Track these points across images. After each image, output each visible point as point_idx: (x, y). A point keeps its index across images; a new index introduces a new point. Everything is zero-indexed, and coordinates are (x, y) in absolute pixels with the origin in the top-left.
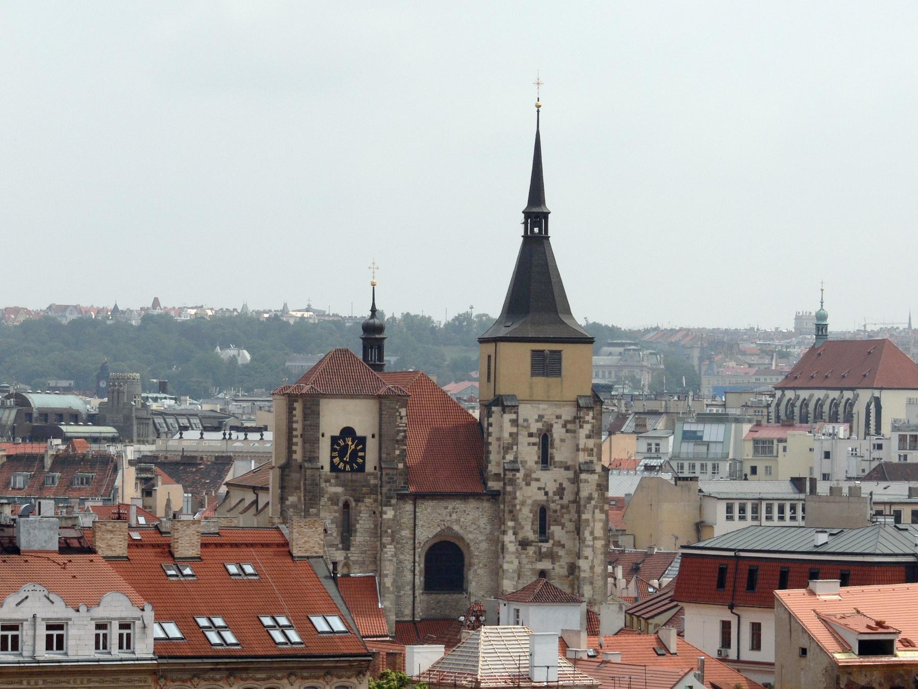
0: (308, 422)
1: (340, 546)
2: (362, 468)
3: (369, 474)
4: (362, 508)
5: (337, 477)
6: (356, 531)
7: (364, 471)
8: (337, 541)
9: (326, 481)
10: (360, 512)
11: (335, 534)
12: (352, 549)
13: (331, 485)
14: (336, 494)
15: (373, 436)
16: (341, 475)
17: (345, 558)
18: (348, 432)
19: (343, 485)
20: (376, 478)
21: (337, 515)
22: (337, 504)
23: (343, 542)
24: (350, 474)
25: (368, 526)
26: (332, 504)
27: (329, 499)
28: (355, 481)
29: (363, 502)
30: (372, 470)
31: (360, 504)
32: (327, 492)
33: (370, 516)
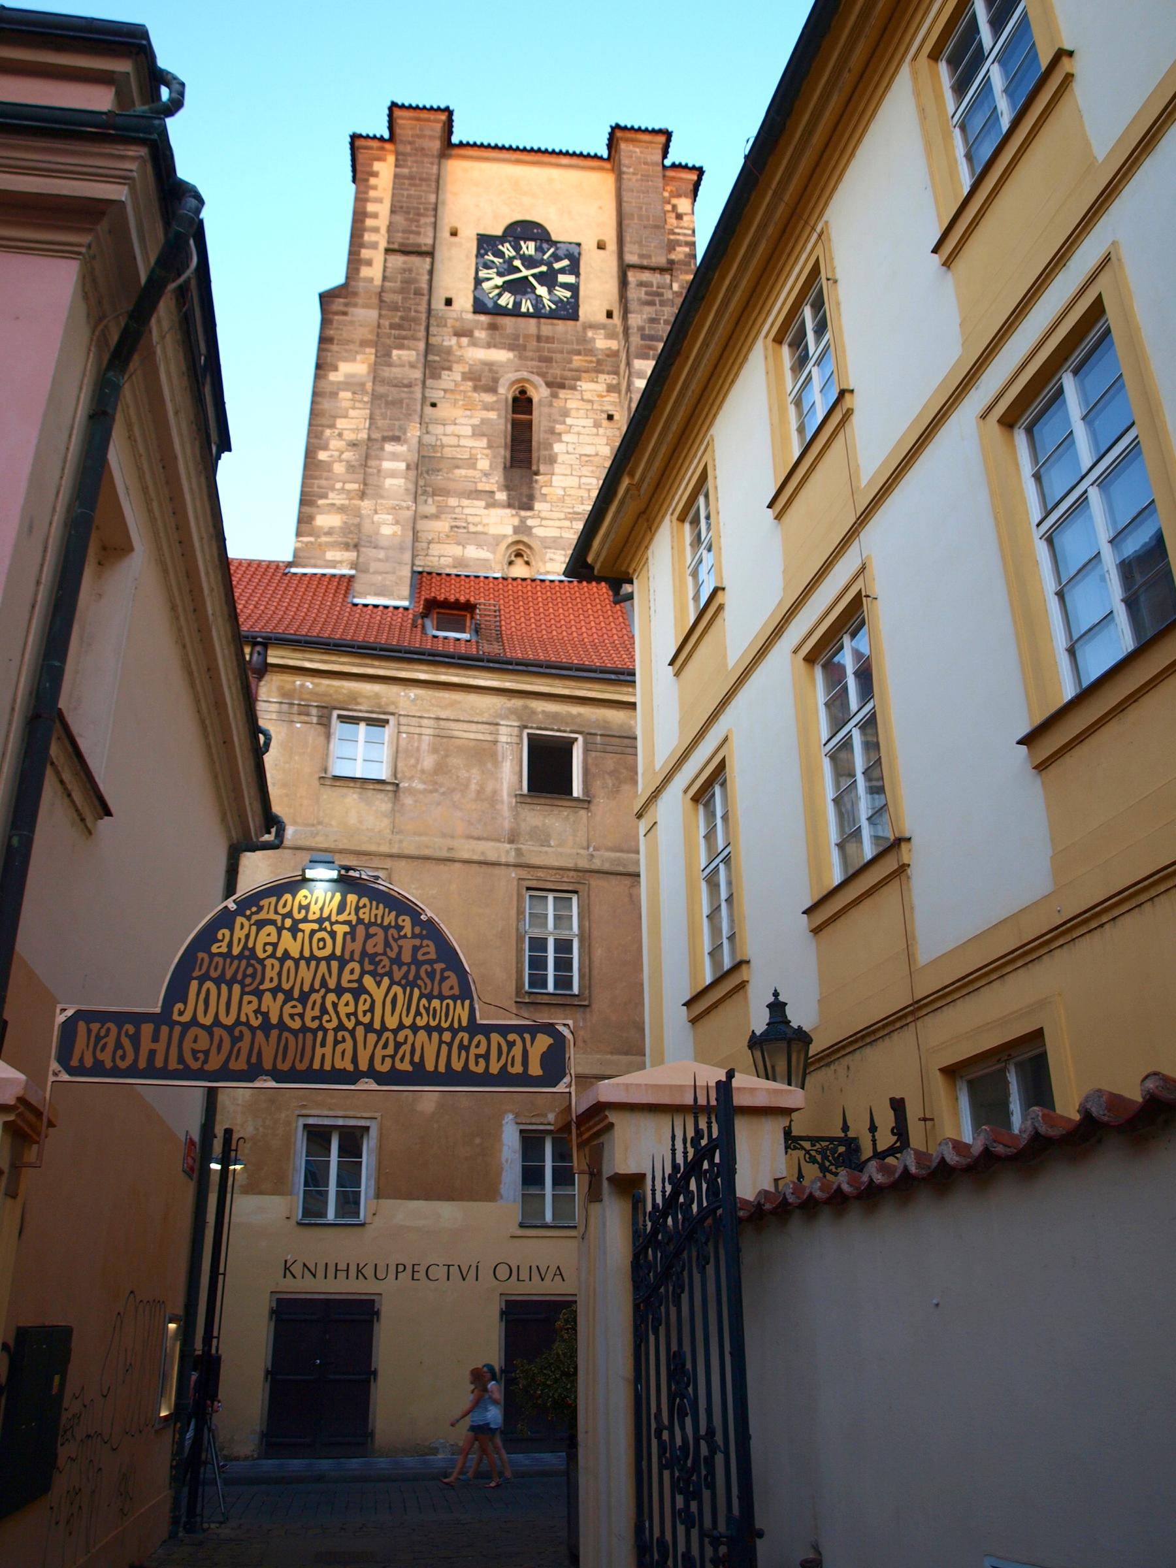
0: (406, 171)
1: (501, 496)
2: (569, 311)
3: (592, 326)
4: (571, 404)
5: (493, 327)
6: (552, 460)
7: (575, 317)
8: (494, 482)
9: (458, 334)
10: (565, 413)
11: (484, 464)
12: (538, 506)
13: (474, 344)
14: (490, 365)
15: (601, 246)
16: (508, 322)
17: (517, 530)
18: (522, 230)
19: (513, 345)
20: (611, 336)
21: (493, 415)
22: (493, 390)
24: (533, 321)
25: (589, 450)
26: (476, 389)
27: (466, 377)
29: (574, 388)
30: (601, 317)
31: (562, 394)
32: (460, 360)
33: (597, 425)
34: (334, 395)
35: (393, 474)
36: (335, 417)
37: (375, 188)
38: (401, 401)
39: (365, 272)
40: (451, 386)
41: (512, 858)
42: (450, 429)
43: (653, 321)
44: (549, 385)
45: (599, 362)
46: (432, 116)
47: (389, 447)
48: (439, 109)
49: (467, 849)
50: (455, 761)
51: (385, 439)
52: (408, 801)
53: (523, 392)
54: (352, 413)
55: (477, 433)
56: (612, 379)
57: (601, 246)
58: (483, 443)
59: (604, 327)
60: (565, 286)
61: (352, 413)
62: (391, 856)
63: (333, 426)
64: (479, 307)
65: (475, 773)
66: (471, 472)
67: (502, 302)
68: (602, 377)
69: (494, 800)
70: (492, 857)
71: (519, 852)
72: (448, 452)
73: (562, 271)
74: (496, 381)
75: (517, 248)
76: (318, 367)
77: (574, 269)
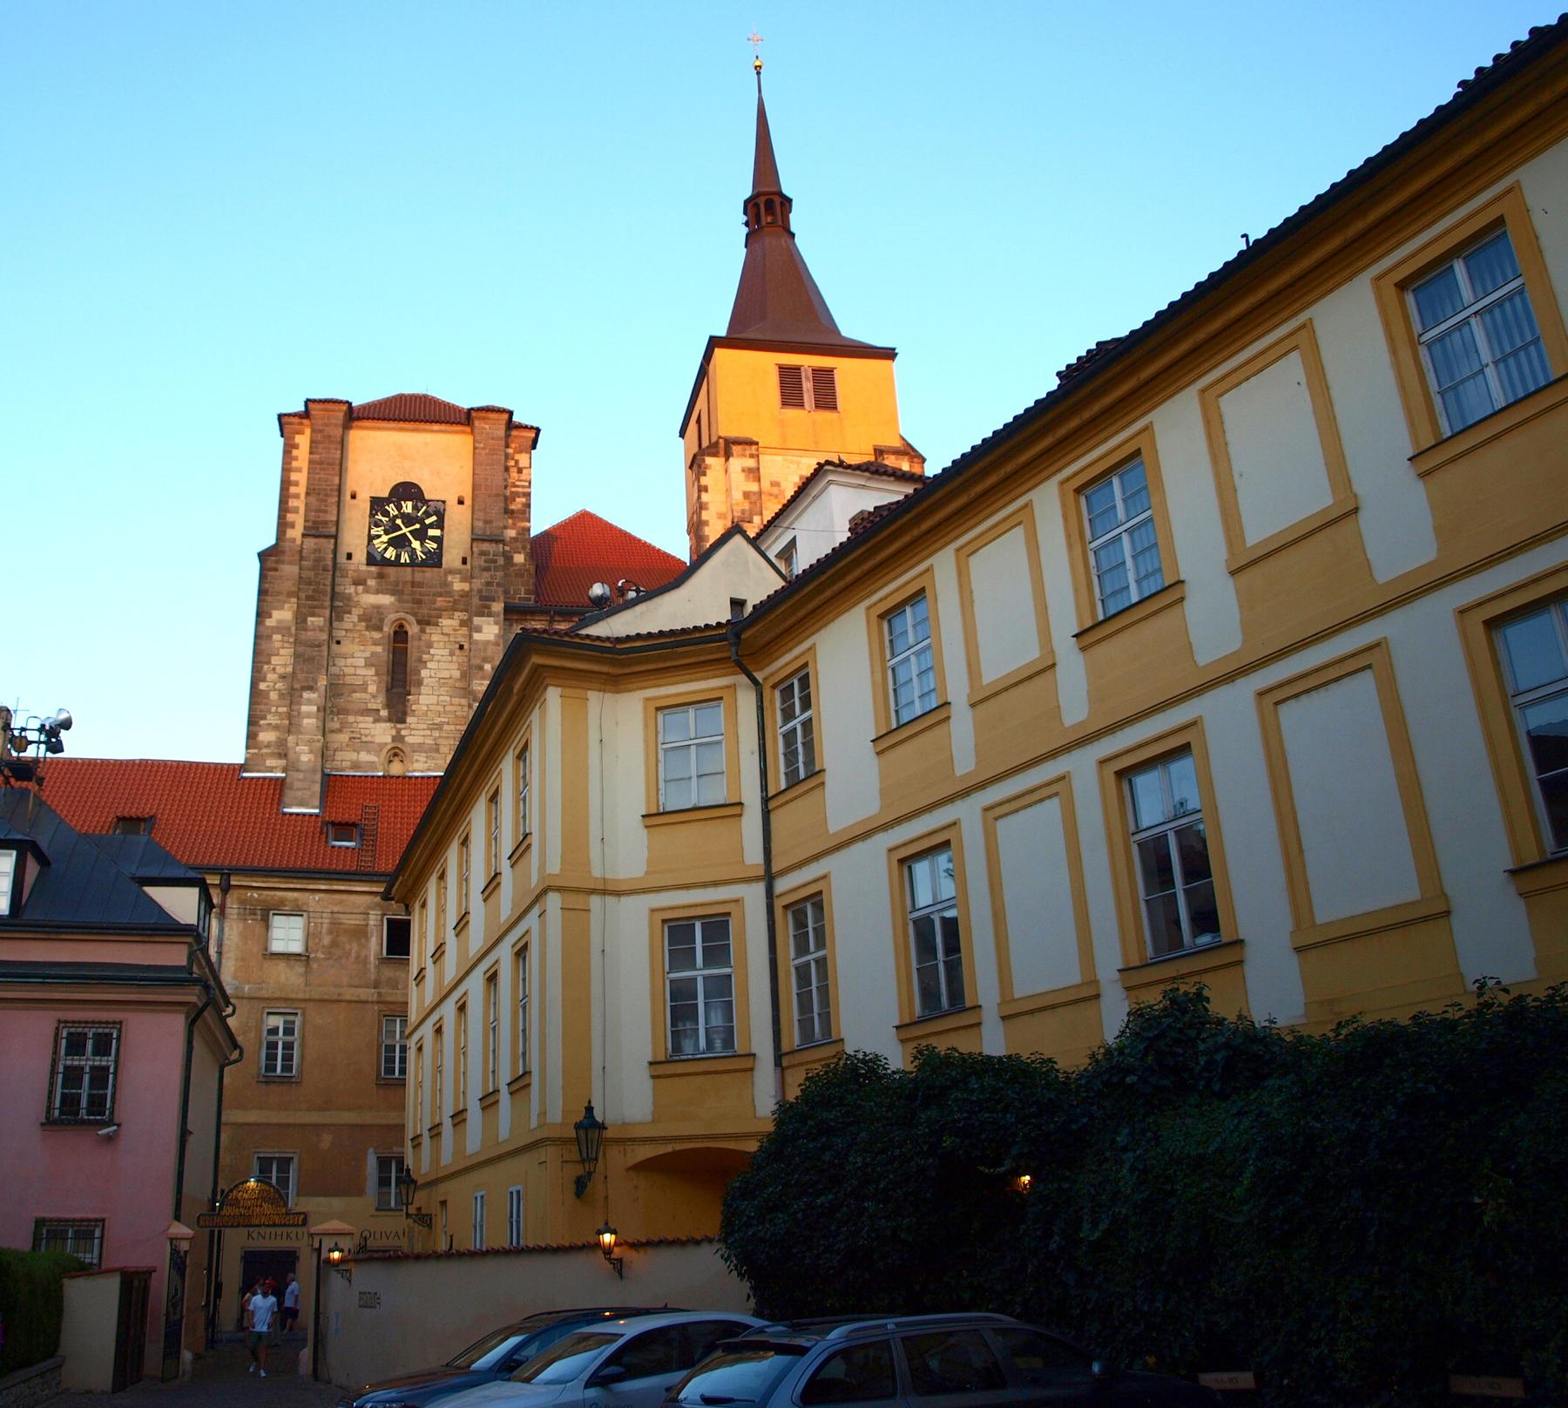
0: (317, 457)
1: (384, 713)
2: (434, 559)
3: (451, 572)
4: (434, 638)
5: (381, 576)
6: (420, 683)
7: (439, 565)
8: (378, 703)
9: (356, 583)
10: (430, 645)
11: (372, 688)
12: (409, 720)
13: (367, 591)
14: (378, 607)
15: (461, 502)
16: (391, 570)
17: (394, 739)
18: (406, 490)
21: (379, 649)
22: (379, 628)
23: (389, 705)
24: (409, 570)
25: (446, 674)
26: (368, 628)
27: (361, 618)
28: (420, 585)
30: (458, 564)
31: (428, 629)
32: (357, 604)
33: (452, 654)
34: (270, 637)
35: (309, 716)
36: (270, 655)
37: (296, 459)
38: (313, 658)
39: (290, 533)
40: (350, 626)
41: (375, 998)
42: (350, 661)
43: (488, 584)
44: (419, 622)
45: (455, 602)
46: (336, 407)
47: (306, 695)
48: (341, 402)
49: (349, 994)
50: (343, 939)
51: (304, 688)
52: (315, 966)
53: (401, 626)
54: (282, 652)
55: (368, 665)
56: (463, 616)
57: (461, 502)
58: (372, 671)
59: (459, 572)
60: (433, 539)
61: (282, 652)
62: (305, 1000)
63: (269, 663)
64: (371, 560)
65: (355, 946)
66: (363, 695)
67: (387, 555)
68: (457, 614)
69: (365, 961)
70: (363, 998)
71: (379, 994)
72: (348, 680)
73: (431, 526)
74: (382, 620)
75: (399, 508)
76: (259, 615)
77: (440, 525)
